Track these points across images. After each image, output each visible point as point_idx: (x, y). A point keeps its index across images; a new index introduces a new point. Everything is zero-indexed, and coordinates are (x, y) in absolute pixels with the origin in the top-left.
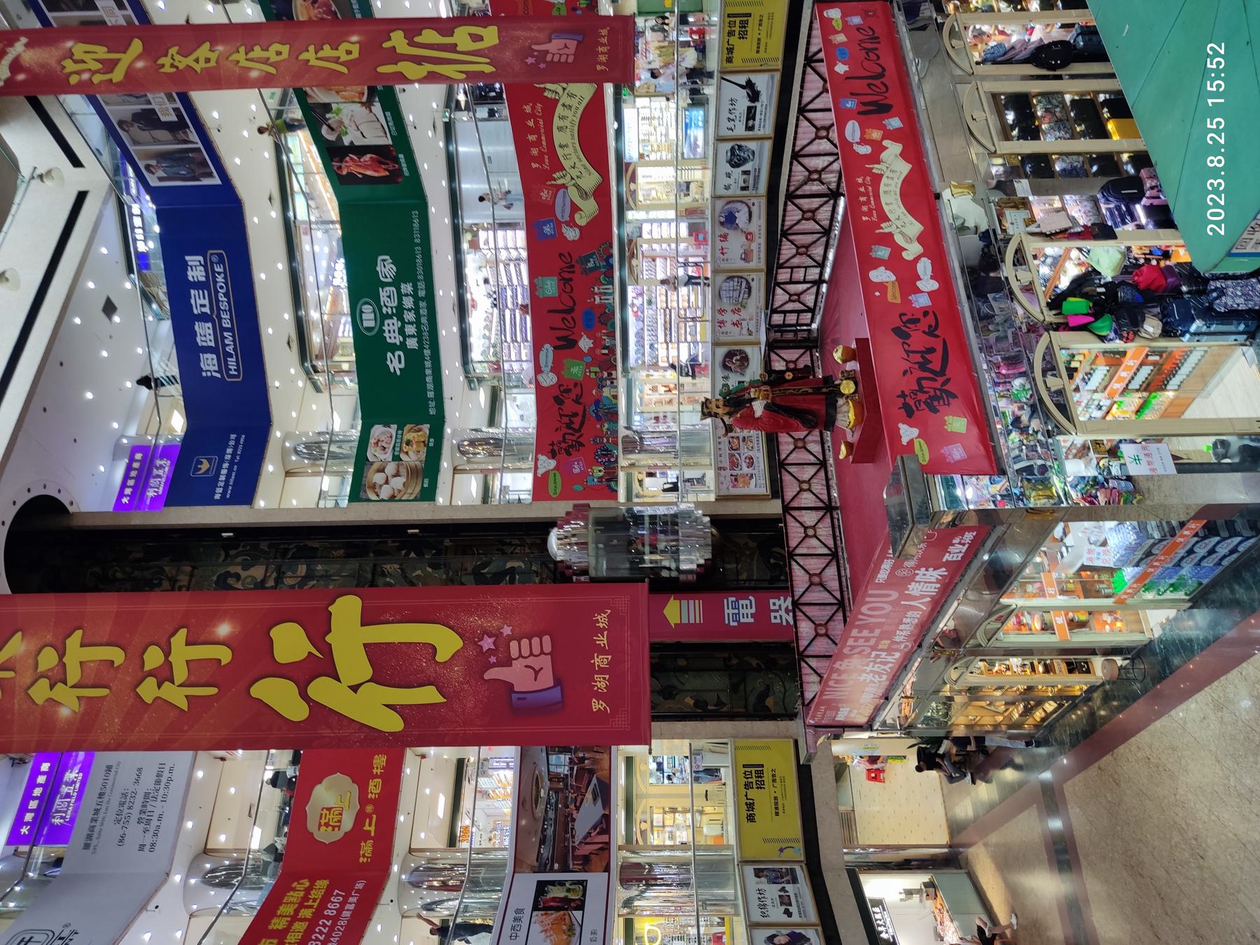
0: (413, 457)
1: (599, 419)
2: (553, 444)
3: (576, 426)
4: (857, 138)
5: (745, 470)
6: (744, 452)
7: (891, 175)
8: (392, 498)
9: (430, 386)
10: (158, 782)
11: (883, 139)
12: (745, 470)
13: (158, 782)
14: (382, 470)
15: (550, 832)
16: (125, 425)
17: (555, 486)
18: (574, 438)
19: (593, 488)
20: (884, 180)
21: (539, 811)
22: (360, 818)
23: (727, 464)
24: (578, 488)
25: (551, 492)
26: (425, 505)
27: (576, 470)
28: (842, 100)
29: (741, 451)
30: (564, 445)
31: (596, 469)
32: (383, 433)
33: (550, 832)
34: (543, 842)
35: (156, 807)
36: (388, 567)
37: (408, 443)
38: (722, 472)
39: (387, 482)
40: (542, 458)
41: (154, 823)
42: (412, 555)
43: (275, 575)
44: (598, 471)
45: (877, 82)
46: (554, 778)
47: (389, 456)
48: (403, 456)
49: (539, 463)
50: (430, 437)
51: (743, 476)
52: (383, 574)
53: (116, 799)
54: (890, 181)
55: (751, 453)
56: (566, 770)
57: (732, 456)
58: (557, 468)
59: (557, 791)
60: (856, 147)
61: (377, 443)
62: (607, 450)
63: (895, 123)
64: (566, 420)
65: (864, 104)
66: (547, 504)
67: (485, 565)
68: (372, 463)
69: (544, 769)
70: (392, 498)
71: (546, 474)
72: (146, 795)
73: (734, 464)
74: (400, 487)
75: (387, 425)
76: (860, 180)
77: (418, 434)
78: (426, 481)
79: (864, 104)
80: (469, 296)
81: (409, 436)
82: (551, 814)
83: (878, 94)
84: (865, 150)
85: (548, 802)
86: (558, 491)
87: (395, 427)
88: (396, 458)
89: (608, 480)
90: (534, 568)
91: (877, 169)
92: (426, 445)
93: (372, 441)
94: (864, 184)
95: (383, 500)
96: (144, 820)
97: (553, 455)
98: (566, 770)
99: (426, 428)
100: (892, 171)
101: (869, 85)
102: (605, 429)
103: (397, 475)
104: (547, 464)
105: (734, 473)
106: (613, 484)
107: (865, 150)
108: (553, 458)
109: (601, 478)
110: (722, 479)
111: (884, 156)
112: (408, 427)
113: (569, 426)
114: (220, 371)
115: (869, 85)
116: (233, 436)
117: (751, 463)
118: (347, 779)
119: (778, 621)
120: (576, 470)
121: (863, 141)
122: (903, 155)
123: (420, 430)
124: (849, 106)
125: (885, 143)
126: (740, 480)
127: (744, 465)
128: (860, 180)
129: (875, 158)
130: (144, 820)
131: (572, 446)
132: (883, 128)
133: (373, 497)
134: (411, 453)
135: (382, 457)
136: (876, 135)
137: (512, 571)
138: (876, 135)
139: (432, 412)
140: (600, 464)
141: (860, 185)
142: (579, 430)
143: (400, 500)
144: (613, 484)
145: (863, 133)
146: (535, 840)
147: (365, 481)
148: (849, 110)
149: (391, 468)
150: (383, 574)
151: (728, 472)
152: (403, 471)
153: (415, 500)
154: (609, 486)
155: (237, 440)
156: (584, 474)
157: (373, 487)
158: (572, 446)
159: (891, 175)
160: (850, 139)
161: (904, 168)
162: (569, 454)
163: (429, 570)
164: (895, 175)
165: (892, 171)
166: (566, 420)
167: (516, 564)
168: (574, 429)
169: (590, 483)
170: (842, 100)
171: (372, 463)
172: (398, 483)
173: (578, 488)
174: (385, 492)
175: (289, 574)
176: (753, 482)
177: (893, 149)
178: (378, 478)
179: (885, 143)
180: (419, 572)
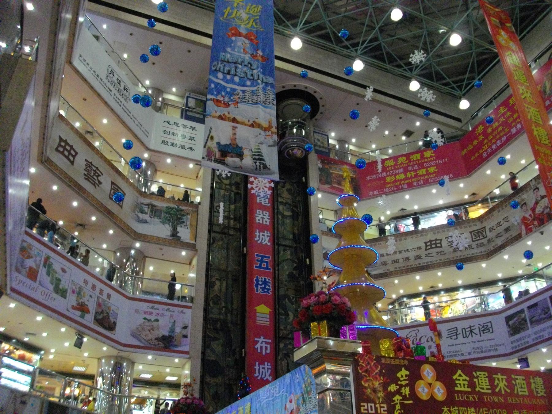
16: (354, 145)
36: (288, 252)
42: (295, 265)
43: (284, 201)
52: (284, 250)
67: (290, 300)
80: (436, 214)
90: (288, 326)
119: (258, 213)
137: (288, 315)
150: (284, 250)
163: (287, 273)
167: (291, 316)
175: (285, 208)
180: (286, 267)
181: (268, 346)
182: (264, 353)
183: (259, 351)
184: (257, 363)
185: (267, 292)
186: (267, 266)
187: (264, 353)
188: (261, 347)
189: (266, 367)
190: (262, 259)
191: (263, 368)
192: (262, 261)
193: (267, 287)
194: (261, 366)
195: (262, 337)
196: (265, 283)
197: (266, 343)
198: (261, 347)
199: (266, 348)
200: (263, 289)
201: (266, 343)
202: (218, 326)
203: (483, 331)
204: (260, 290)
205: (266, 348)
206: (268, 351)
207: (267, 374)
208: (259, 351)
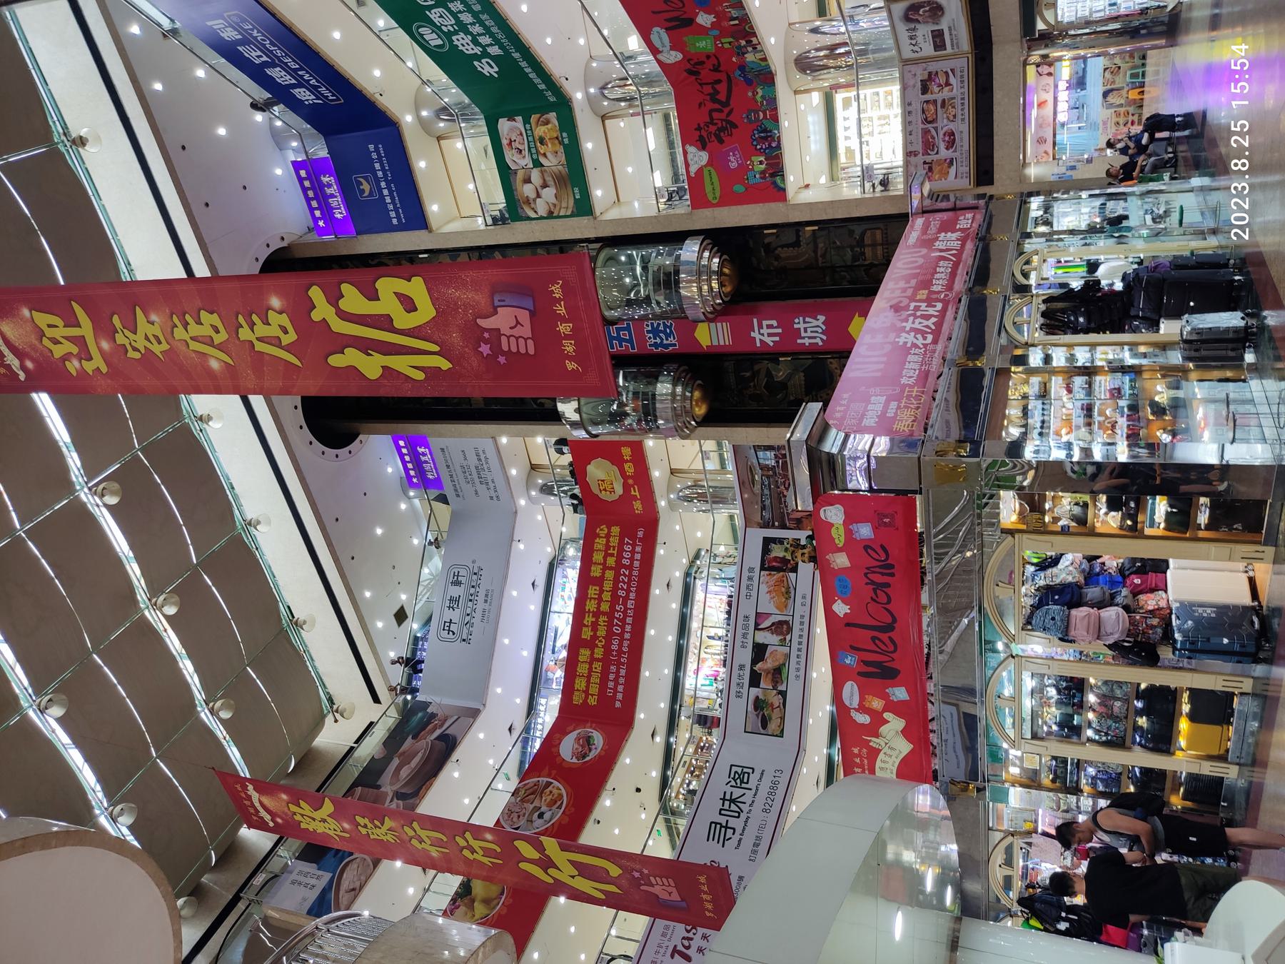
0: (554, 160)
1: (749, 83)
2: (699, 128)
3: (722, 97)
4: (855, 704)
5: (944, 153)
6: (944, 124)
7: (889, 752)
8: (551, 215)
9: (537, 81)
10: (480, 460)
11: (885, 710)
12: (944, 153)
13: (480, 460)
14: (528, 180)
15: (768, 503)
17: (712, 187)
18: (722, 116)
19: (754, 186)
20: (881, 756)
21: (757, 488)
22: (626, 487)
23: (918, 147)
24: (739, 188)
25: (710, 197)
26: (584, 220)
27: (733, 165)
28: (840, 653)
29: (939, 124)
30: (713, 129)
31: (756, 159)
32: (512, 129)
33: (768, 503)
34: (763, 508)
35: (485, 474)
37: (542, 141)
38: (912, 159)
39: (539, 196)
40: (691, 149)
41: (491, 485)
44: (758, 164)
45: (884, 637)
46: (763, 467)
47: (527, 161)
48: (542, 160)
49: (690, 157)
50: (561, 130)
51: (939, 162)
53: (459, 470)
54: (887, 759)
55: (952, 126)
56: (773, 463)
57: (926, 132)
58: (710, 163)
59: (768, 477)
60: (854, 714)
61: (510, 144)
62: (765, 131)
63: (900, 694)
64: (708, 89)
65: (866, 663)
66: (707, 212)
68: (515, 172)
69: (755, 461)
70: (551, 215)
71: (700, 171)
72: (477, 468)
73: (929, 146)
74: (553, 200)
75: (511, 119)
76: (856, 751)
77: (548, 127)
78: (576, 190)
79: (866, 663)
81: (540, 131)
82: (766, 492)
83: (883, 653)
84: (863, 719)
85: (763, 483)
86: (718, 194)
87: (519, 118)
88: (537, 164)
89: (773, 175)
91: (875, 742)
92: (561, 143)
93: (505, 142)
94: (859, 755)
95: (542, 218)
96: (484, 482)
97: (703, 147)
98: (773, 463)
99: (552, 116)
100: (892, 749)
101: (873, 638)
102: (758, 98)
103: (545, 186)
104: (699, 158)
105: (928, 158)
106: (778, 179)
107: (863, 719)
108: (703, 148)
109: (763, 172)
110: (912, 169)
111: (884, 729)
112: (534, 118)
113: (714, 100)
114: (318, 98)
115: (873, 638)
116: (371, 147)
117: (951, 144)
118: (608, 463)
120: (733, 165)
121: (862, 708)
122: (906, 733)
123: (547, 122)
124: (848, 662)
125: (887, 715)
126: (936, 169)
127: (942, 146)
128: (856, 751)
129: (874, 728)
130: (484, 482)
131: (722, 129)
132: (885, 697)
133: (533, 215)
134: (549, 155)
135: (523, 162)
136: (877, 704)
138: (877, 704)
139: (552, 99)
140: (760, 152)
141: (857, 756)
142: (727, 104)
143: (559, 217)
144: (778, 179)
145: (862, 699)
146: (758, 507)
147: (518, 196)
148: (848, 666)
149: (536, 176)
151: (920, 158)
152: (550, 181)
153: (572, 215)
154: (775, 183)
155: (377, 150)
156: (744, 169)
157: (528, 201)
158: (722, 129)
159: (889, 752)
160: (847, 703)
161: (904, 747)
162: (721, 141)
164: (894, 753)
165: (892, 749)
166: (708, 89)
168: (719, 102)
169: (752, 181)
170: (840, 653)
171: (515, 172)
172: (549, 193)
173: (739, 188)
174: (542, 210)
176: (953, 170)
177: (895, 724)
178: (528, 190)
179: (887, 715)
181: (765, 323)
182: (780, 331)
183: (777, 339)
184: (799, 341)
185: (670, 327)
186: (623, 329)
187: (780, 331)
188: (770, 335)
189: (802, 326)
190: (614, 338)
191: (806, 331)
192: (621, 340)
193: (661, 328)
194: (803, 334)
195: (753, 334)
196: (655, 332)
197: (760, 327)
198: (770, 335)
199: (769, 327)
200: (668, 336)
201: (760, 327)
202: (748, 374)
203: (742, 782)
204: (671, 340)
205: (769, 327)
206: (774, 323)
207: (815, 323)
208: (777, 339)
